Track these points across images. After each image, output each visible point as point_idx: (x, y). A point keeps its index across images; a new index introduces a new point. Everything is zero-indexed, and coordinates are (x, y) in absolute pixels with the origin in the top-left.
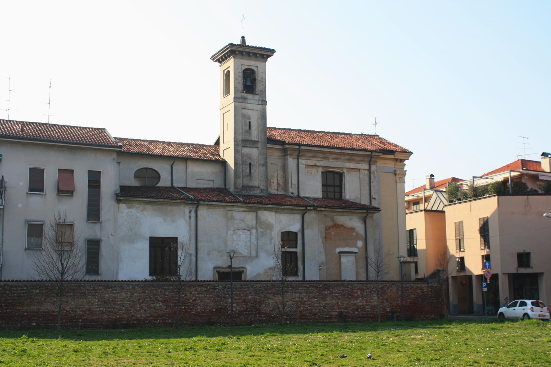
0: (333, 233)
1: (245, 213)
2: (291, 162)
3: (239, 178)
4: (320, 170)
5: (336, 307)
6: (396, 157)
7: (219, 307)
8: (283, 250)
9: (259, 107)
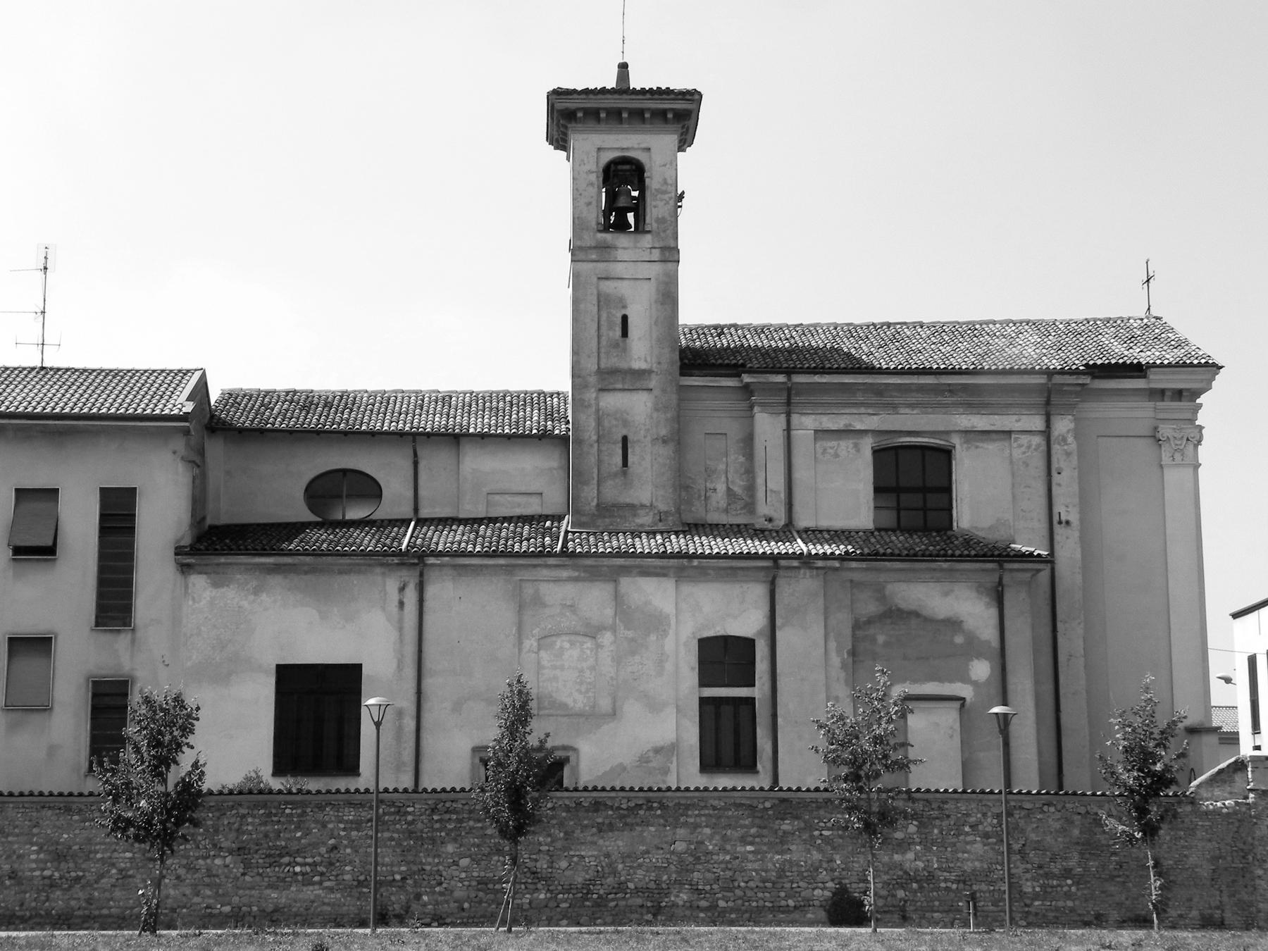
0: (881, 639)
1: (580, 584)
2: (768, 426)
3: (586, 483)
4: (867, 445)
5: (823, 875)
6: (1153, 386)
7: (415, 868)
9: (655, 270)
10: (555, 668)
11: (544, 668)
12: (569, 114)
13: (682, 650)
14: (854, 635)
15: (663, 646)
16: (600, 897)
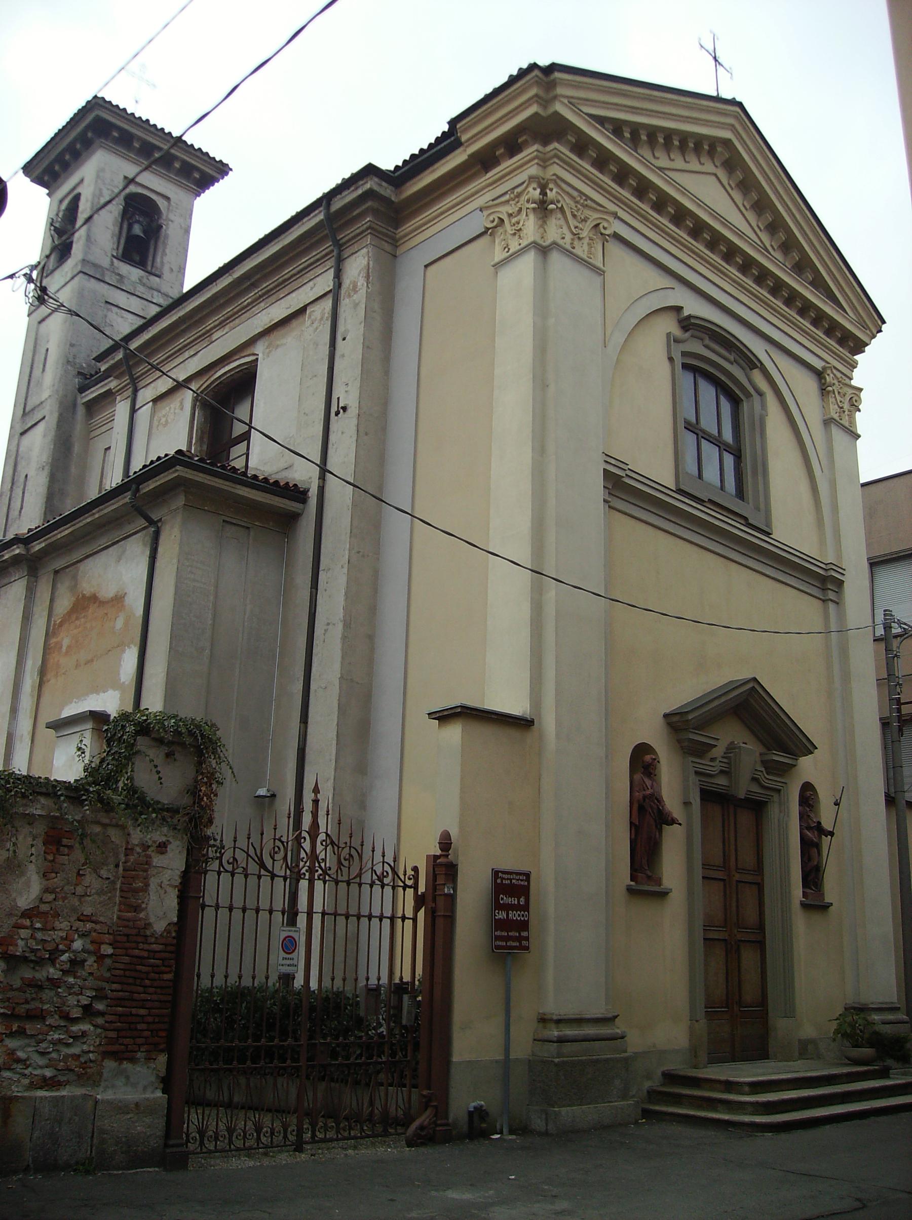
0: (66, 642)
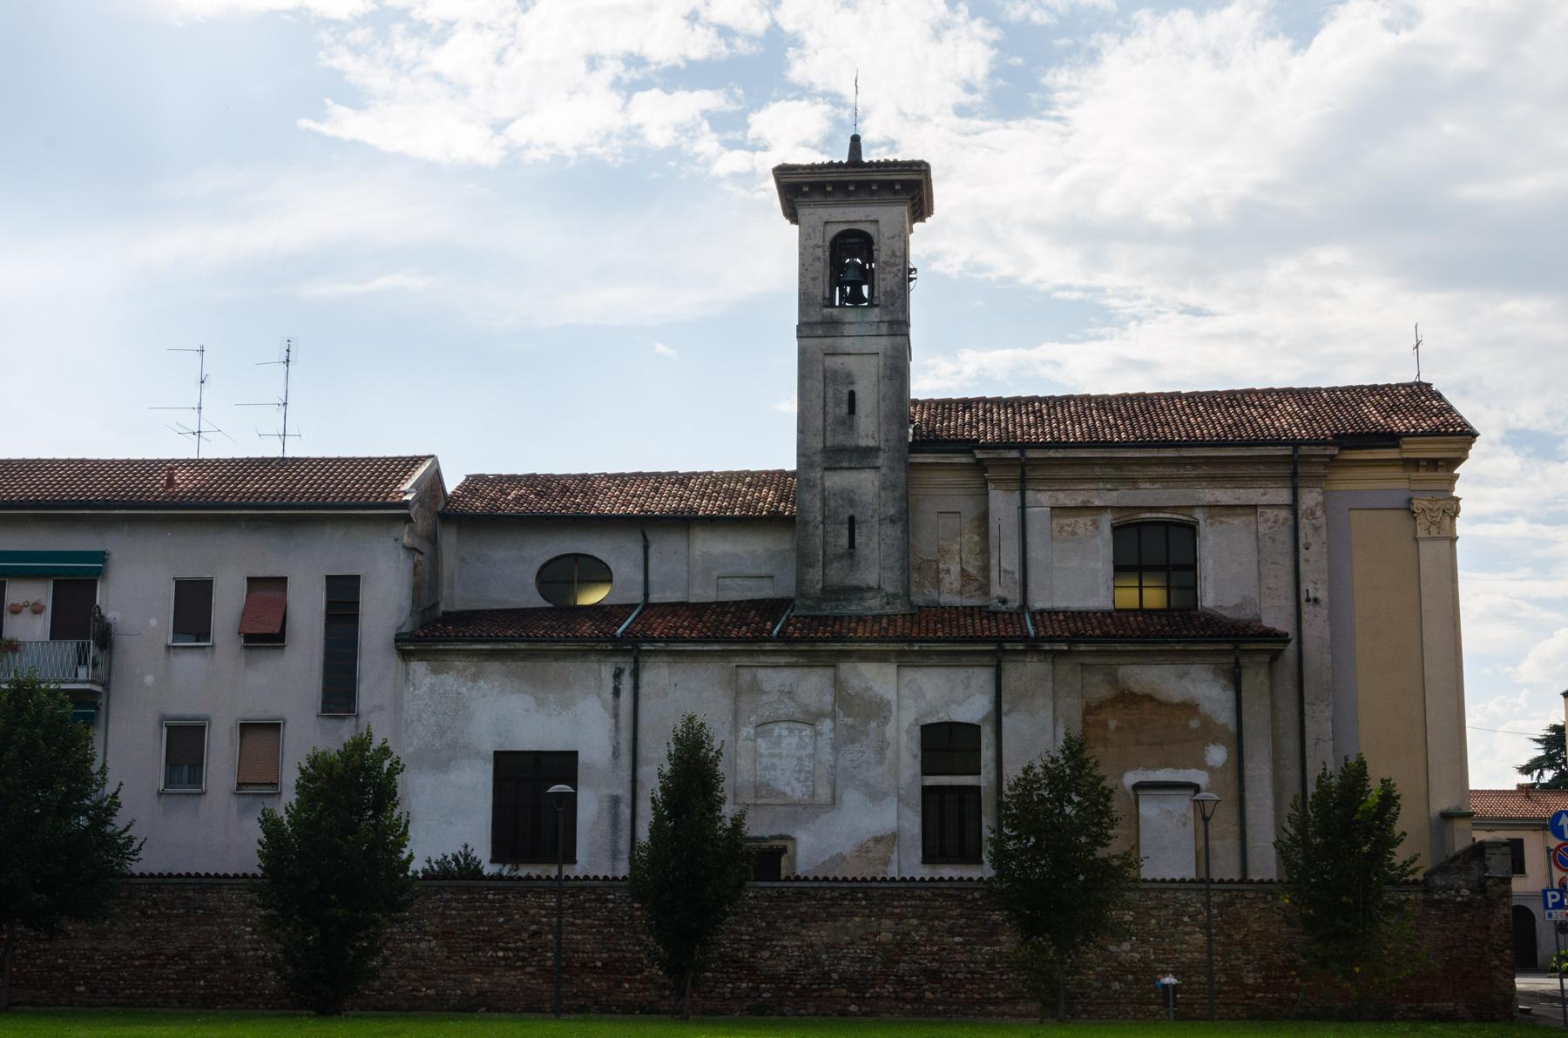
0: (1113, 724)
1: (798, 670)
2: (1002, 503)
3: (811, 565)
4: (1106, 521)
6: (1405, 455)
7: (616, 955)
8: (931, 781)
9: (882, 344)
10: (773, 755)
11: (762, 756)
12: (799, 188)
13: (904, 738)
14: (1084, 721)
15: (884, 734)
16: (803, 987)
